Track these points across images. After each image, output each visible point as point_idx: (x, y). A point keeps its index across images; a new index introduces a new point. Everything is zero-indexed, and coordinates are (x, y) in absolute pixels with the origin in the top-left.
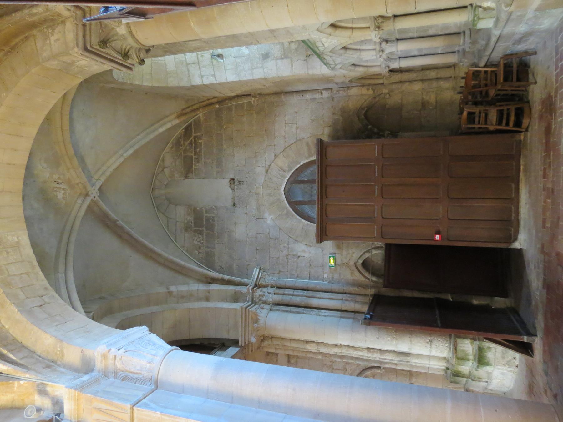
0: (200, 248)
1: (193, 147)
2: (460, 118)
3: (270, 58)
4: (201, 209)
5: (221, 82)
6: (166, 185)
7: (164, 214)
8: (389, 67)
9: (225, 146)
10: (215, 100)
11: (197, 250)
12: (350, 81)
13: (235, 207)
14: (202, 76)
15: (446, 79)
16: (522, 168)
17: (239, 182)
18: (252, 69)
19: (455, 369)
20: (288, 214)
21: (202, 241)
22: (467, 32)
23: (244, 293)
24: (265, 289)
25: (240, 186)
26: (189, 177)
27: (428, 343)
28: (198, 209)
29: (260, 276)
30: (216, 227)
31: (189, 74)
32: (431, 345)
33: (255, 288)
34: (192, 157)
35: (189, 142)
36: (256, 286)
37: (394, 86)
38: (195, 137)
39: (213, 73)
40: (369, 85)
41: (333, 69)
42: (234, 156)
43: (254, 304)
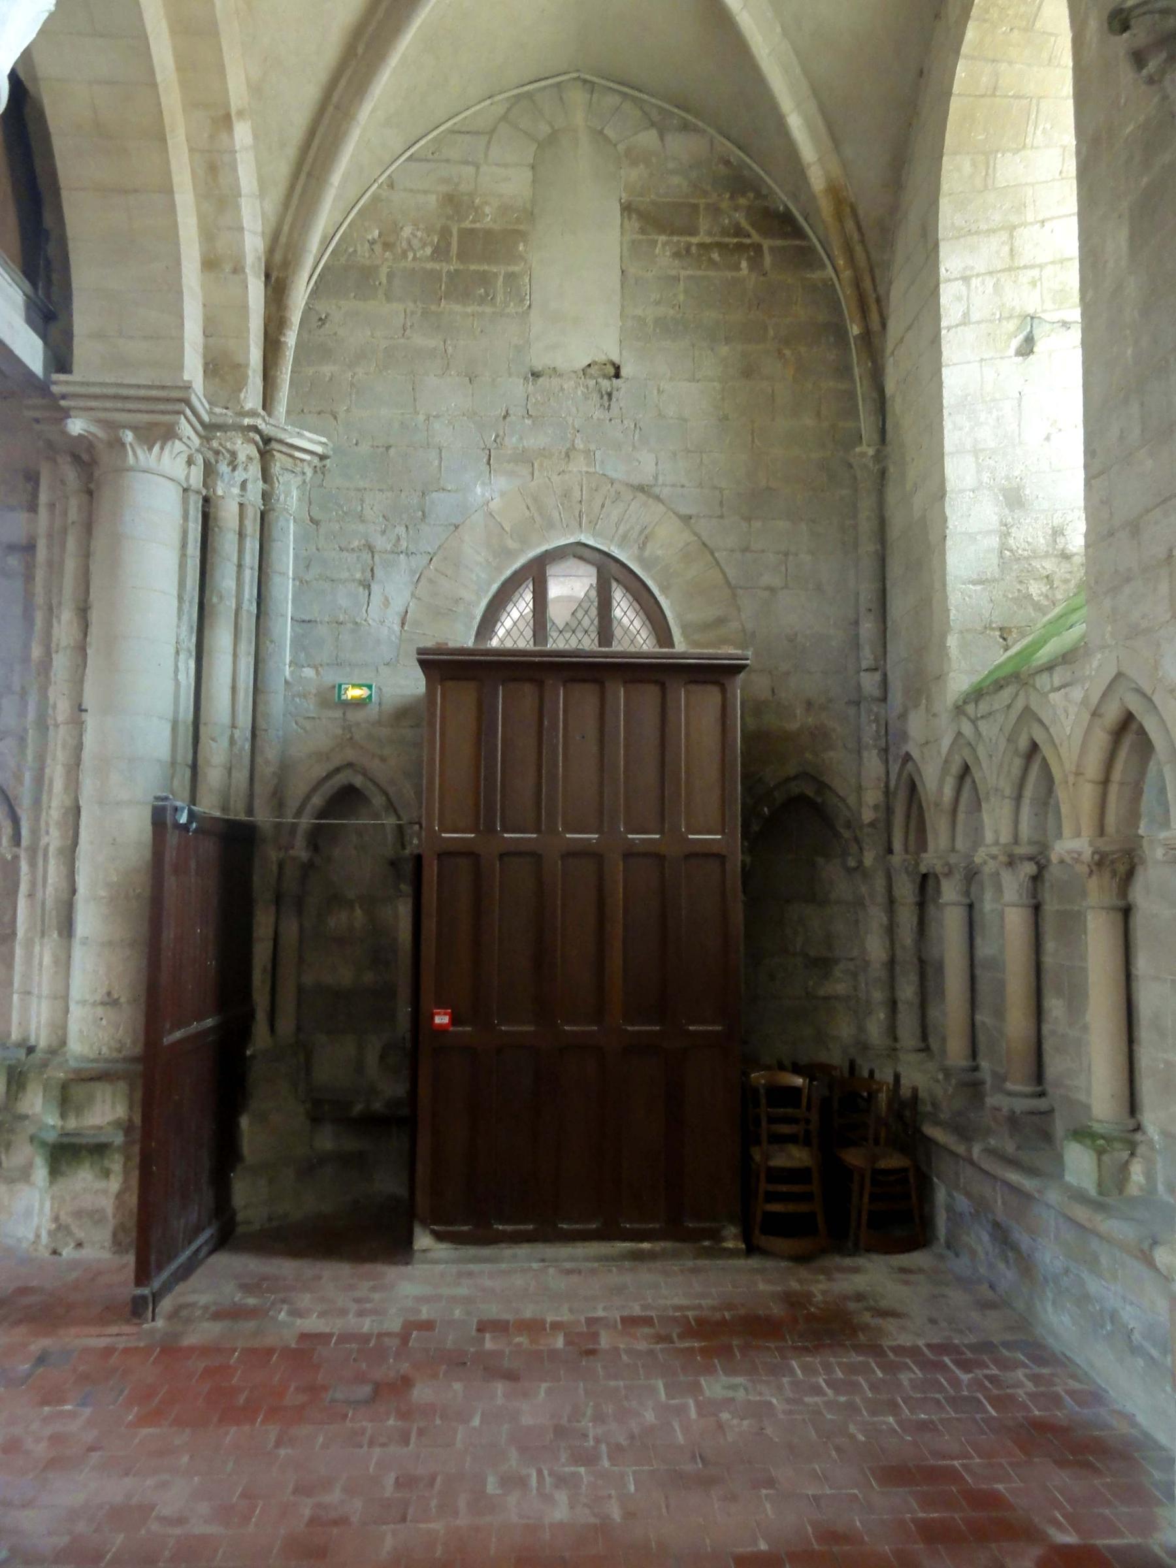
0: (387, 246)
1: (727, 240)
2: (781, 1067)
3: (1007, 511)
4: (521, 257)
5: (943, 342)
6: (601, 132)
7: (504, 118)
8: (949, 874)
9: (724, 350)
10: (875, 325)
11: (380, 236)
12: (908, 758)
13: (525, 378)
14: (966, 279)
15: (892, 1031)
16: (646, 1246)
17: (610, 395)
18: (976, 452)
19: (32, 1075)
21: (410, 255)
22: (1041, 1104)
23: (239, 402)
24: (255, 470)
25: (595, 396)
26: (630, 218)
27: (109, 994)
28: (521, 248)
29: (298, 454)
30: (458, 308)
31: (977, 233)
32: (103, 1004)
33: (257, 438)
34: (693, 232)
35: (744, 224)
36: (267, 440)
37: (880, 883)
38: (758, 248)
39: (975, 316)
40: (889, 810)
41: (959, 710)
42: (693, 379)
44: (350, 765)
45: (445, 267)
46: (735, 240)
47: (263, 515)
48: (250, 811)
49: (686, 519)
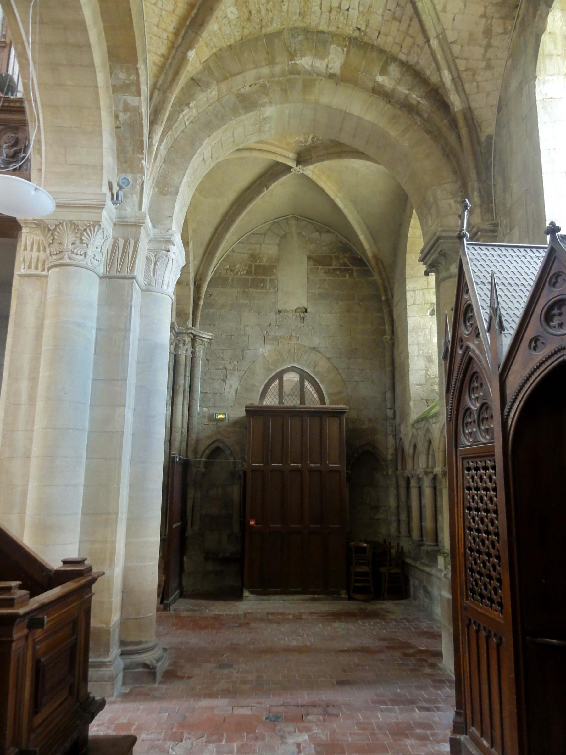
0: (232, 271)
1: (341, 267)
2: (361, 541)
3: (427, 363)
4: (275, 274)
5: (408, 310)
6: (301, 233)
7: (269, 229)
8: (412, 477)
9: (341, 303)
10: (390, 296)
11: (229, 267)
12: (401, 439)
13: (276, 313)
14: (414, 291)
15: (398, 530)
16: (316, 596)
17: (304, 318)
18: (418, 344)
20: (270, 370)
21: (239, 273)
22: (436, 548)
23: (187, 324)
24: (190, 345)
25: (299, 318)
26: (310, 261)
28: (275, 270)
29: (204, 339)
30: (255, 290)
31: (417, 277)
33: (192, 336)
34: (331, 265)
35: (347, 262)
36: (194, 336)
37: (394, 480)
38: (352, 270)
39: (417, 302)
40: (396, 455)
41: (413, 425)
42: (330, 313)
43: (175, 334)
44: (218, 440)
45: (251, 277)
46: (344, 267)
47: (192, 359)
48: (187, 456)
49: (329, 359)
